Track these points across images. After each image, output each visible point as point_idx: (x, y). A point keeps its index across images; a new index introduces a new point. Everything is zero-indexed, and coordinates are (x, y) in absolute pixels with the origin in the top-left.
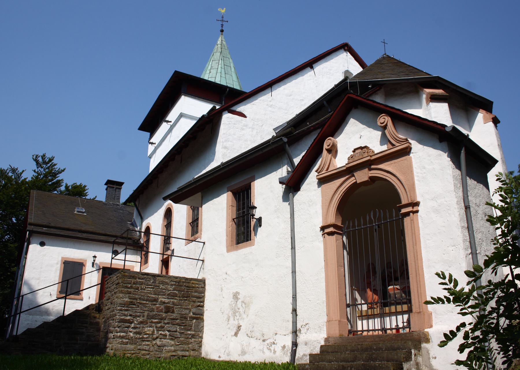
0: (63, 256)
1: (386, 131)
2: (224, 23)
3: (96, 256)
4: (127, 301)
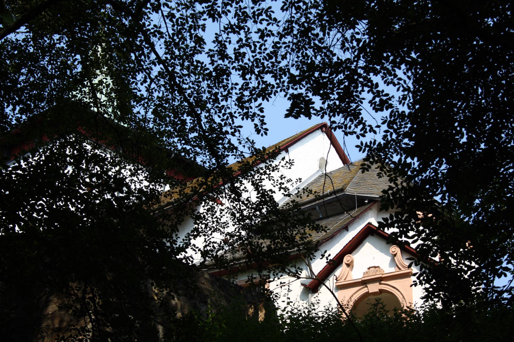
1: (395, 258)
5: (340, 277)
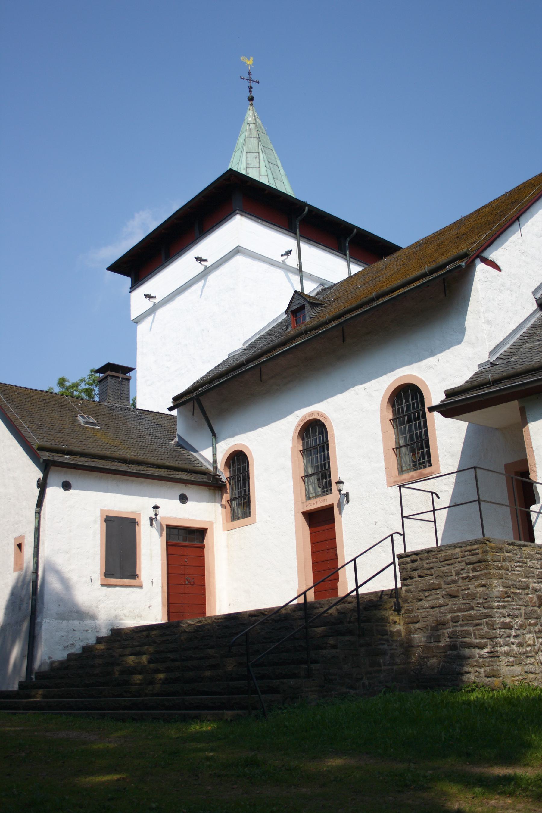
0: (102, 508)
2: (253, 85)
3: (159, 505)
4: (502, 591)
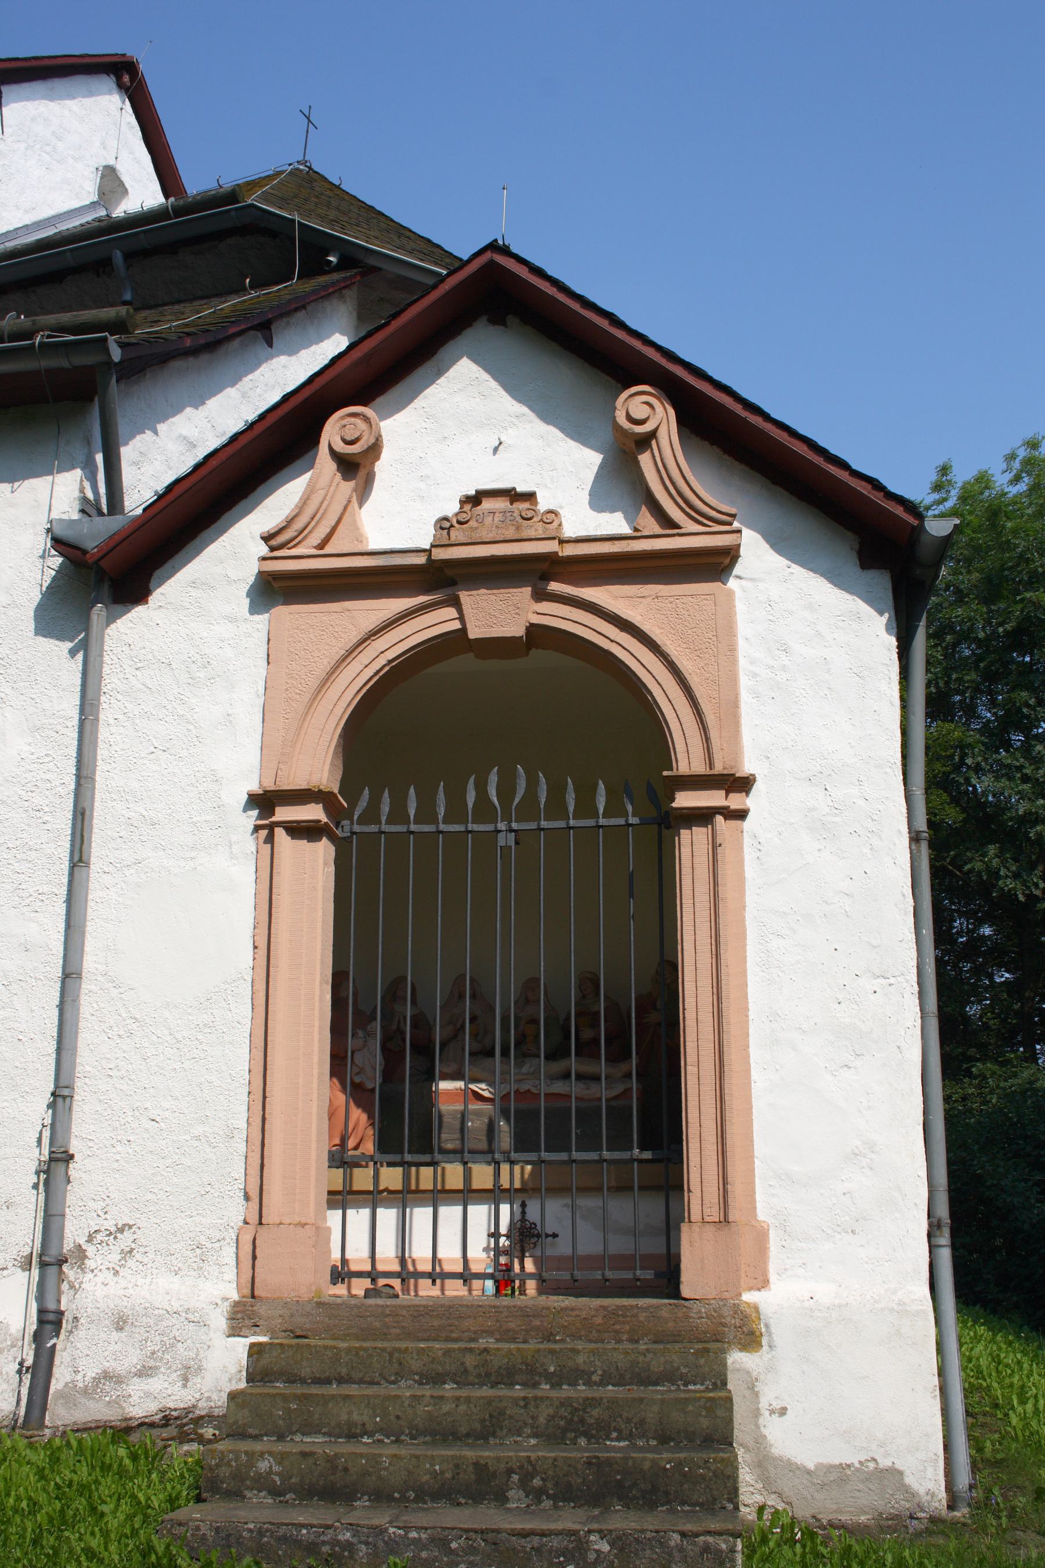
1: (645, 460)
5: (298, 525)
